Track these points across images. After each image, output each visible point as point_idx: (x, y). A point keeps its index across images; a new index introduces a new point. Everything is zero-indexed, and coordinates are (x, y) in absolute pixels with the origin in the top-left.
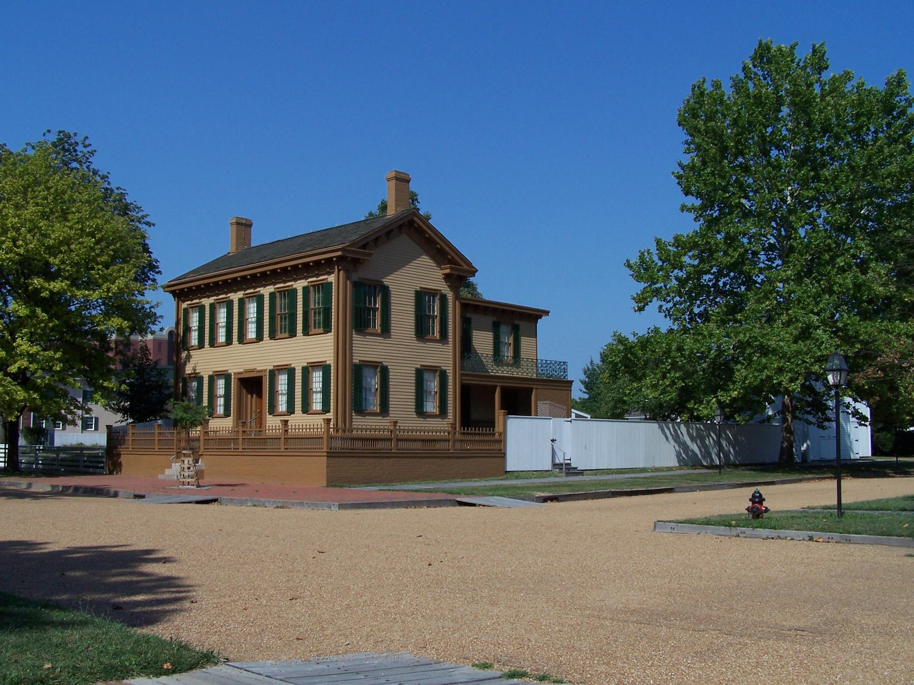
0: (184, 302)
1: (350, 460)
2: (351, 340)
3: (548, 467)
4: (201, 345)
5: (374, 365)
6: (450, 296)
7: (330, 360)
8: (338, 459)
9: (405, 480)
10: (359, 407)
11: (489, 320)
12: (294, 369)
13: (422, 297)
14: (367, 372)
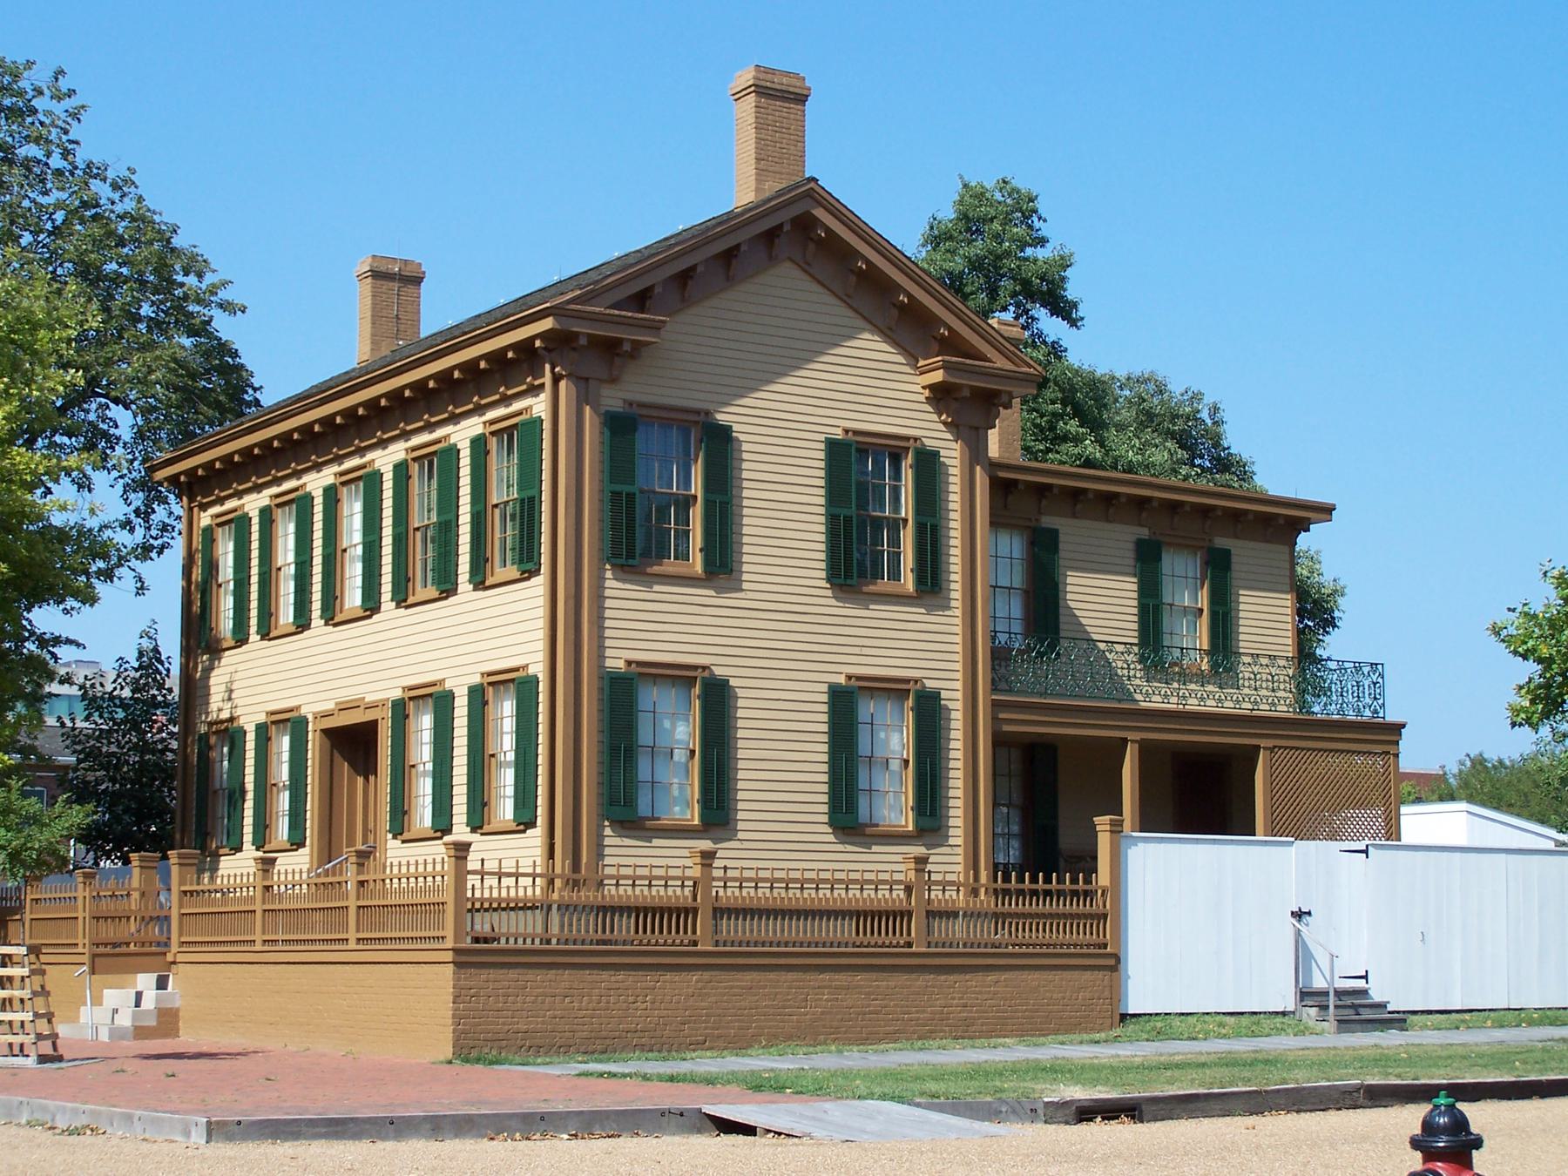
0: (204, 507)
1: (539, 976)
2: (599, 598)
3: (1285, 999)
4: (241, 640)
5: (679, 676)
6: (952, 454)
7: (538, 667)
8: (493, 974)
9: (740, 1043)
10: (624, 808)
11: (1123, 536)
12: (449, 697)
13: (854, 466)
14: (651, 697)
